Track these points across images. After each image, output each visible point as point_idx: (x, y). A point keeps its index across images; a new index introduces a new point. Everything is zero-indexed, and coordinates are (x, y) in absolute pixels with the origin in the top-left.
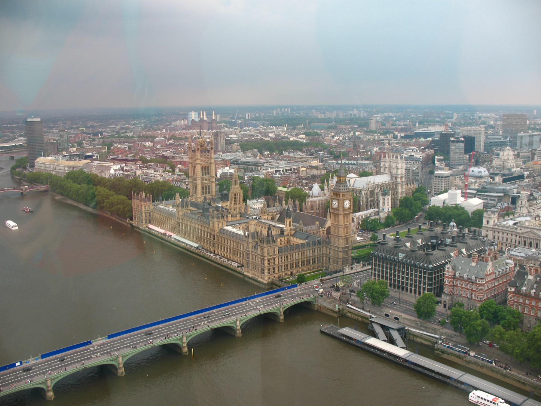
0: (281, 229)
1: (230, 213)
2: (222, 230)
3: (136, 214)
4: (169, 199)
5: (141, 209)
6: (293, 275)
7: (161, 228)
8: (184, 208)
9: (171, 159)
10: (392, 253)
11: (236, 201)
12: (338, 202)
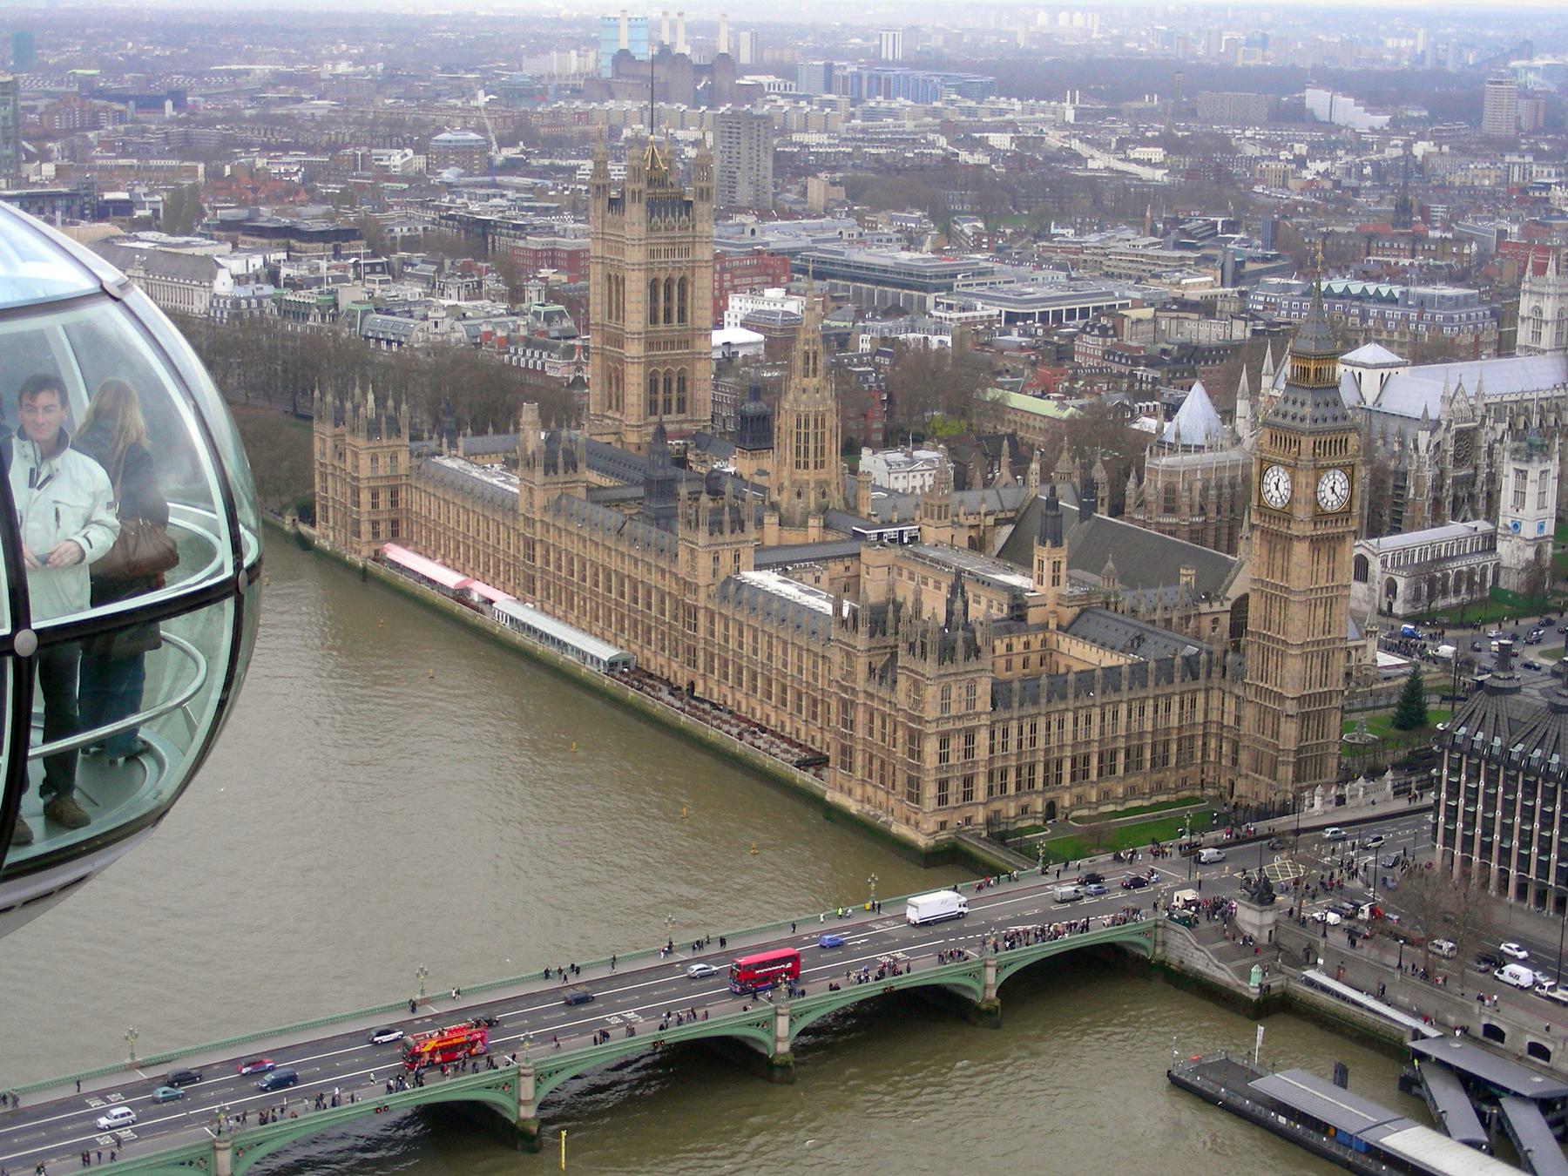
0: (1015, 597)
1: (774, 507)
2: (732, 587)
4: (490, 430)
5: (356, 467)
6: (1060, 817)
7: (445, 564)
8: (556, 473)
9: (508, 235)
10: (1538, 734)
11: (807, 449)
12: (1293, 479)
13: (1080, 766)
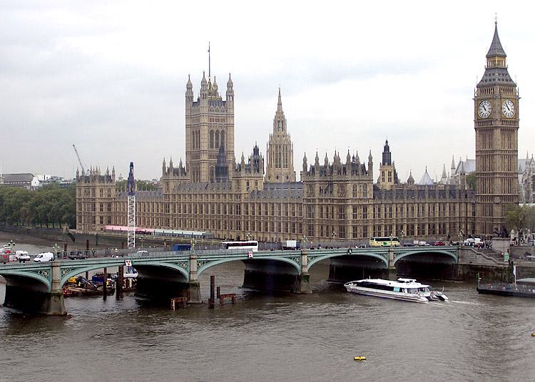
3: (81, 209)
5: (94, 194)
13: (410, 228)
